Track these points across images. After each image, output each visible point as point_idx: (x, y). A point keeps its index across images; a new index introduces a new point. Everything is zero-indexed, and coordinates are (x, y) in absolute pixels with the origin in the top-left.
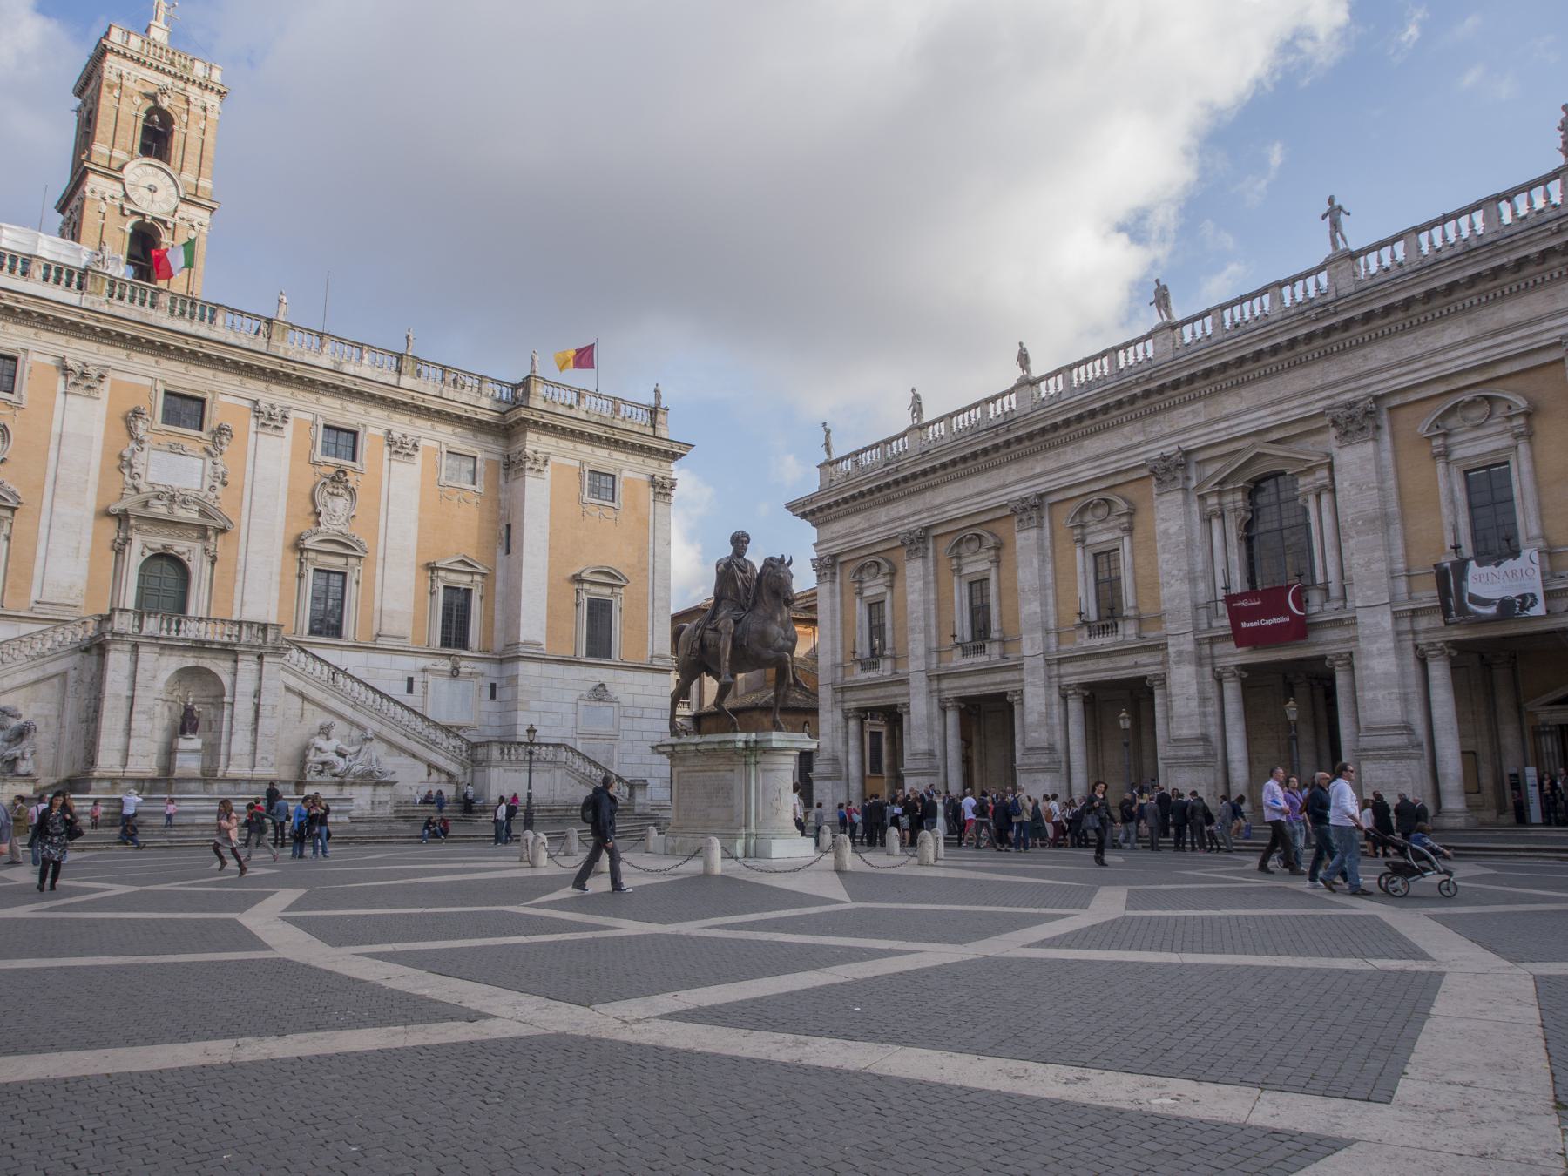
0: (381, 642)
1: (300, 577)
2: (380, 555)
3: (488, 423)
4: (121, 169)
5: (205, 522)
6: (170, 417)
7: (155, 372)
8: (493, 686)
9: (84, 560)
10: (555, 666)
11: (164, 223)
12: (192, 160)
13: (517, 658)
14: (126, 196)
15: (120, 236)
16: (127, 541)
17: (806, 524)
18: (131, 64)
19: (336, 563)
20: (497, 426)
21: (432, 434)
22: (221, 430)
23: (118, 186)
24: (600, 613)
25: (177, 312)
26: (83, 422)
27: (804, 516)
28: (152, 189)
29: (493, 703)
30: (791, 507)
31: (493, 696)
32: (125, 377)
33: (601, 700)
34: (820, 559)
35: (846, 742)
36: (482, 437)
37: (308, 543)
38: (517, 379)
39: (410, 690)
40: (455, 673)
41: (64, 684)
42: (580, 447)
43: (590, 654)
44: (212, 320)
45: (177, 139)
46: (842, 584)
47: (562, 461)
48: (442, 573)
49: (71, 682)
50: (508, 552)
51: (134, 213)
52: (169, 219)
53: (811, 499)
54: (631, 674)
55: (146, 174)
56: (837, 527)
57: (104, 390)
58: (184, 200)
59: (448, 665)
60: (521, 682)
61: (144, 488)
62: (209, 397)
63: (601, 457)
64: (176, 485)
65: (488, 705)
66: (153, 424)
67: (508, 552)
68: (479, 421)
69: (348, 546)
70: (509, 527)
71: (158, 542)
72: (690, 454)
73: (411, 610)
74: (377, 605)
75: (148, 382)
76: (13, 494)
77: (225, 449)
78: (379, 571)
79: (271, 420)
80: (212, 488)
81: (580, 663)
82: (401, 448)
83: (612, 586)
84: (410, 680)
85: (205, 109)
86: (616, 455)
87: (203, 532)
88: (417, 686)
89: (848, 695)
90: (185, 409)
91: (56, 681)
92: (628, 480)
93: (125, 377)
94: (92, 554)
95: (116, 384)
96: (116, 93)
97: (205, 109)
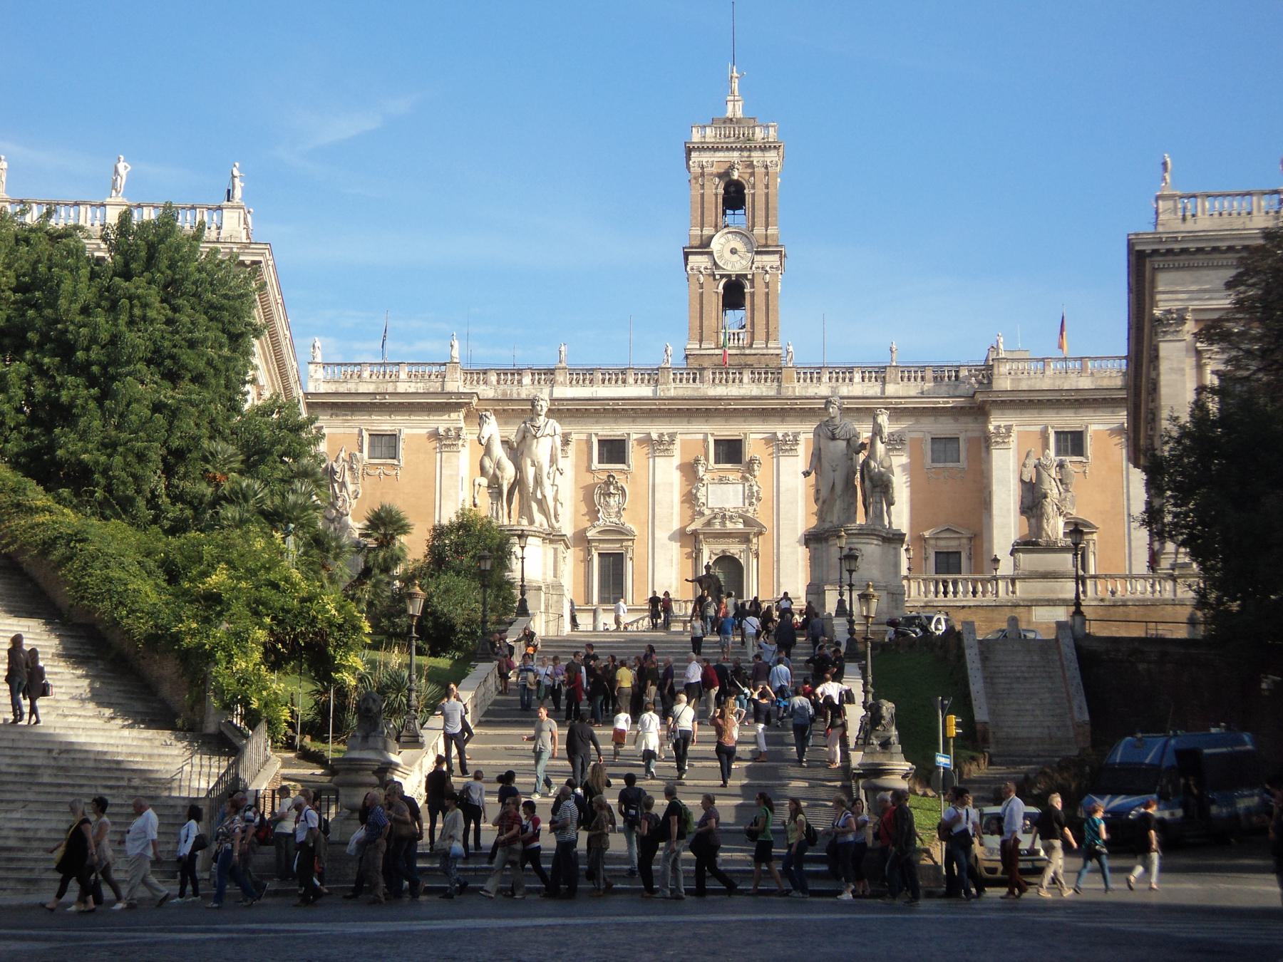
3: (962, 408)
4: (708, 245)
5: (748, 530)
11: (746, 276)
12: (760, 214)
14: (715, 264)
15: (715, 297)
18: (708, 154)
22: (752, 461)
25: (717, 381)
26: (668, 472)
28: (734, 251)
32: (689, 437)
36: (962, 419)
44: (741, 381)
45: (748, 199)
48: (932, 542)
51: (722, 276)
55: (728, 241)
57: (677, 449)
58: (758, 253)
61: (707, 512)
63: (1069, 420)
64: (727, 506)
66: (710, 468)
71: (719, 548)
76: (631, 532)
77: (757, 473)
80: (751, 504)
85: (766, 167)
87: (745, 538)
90: (731, 451)
97: (766, 167)
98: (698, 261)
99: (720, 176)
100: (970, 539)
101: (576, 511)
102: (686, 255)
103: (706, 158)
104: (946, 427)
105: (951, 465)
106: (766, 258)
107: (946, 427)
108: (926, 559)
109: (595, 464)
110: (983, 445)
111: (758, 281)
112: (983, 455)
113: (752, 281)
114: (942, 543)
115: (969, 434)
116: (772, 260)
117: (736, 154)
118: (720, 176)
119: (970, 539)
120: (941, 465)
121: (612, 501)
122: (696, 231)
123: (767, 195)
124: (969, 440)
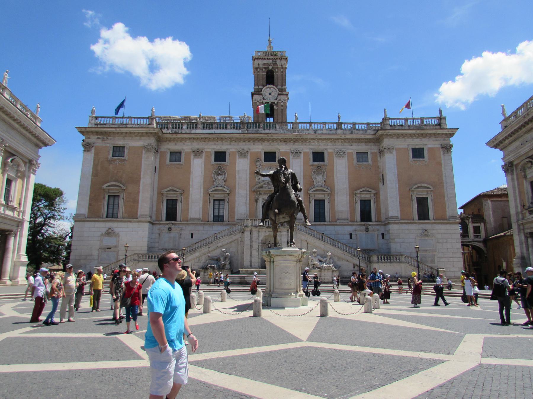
0: (338, 222)
1: (310, 203)
2: (336, 192)
3: (370, 139)
4: (261, 91)
6: (266, 160)
7: (261, 147)
8: (383, 235)
9: (248, 206)
10: (405, 225)
11: (274, 102)
13: (388, 223)
14: (263, 98)
16: (258, 198)
17: (497, 150)
18: (261, 60)
19: (320, 197)
20: (373, 139)
21: (351, 147)
23: (261, 96)
24: (422, 203)
27: (496, 147)
28: (270, 94)
29: (383, 240)
30: (488, 144)
31: (383, 238)
33: (427, 236)
34: (505, 165)
35: (527, 249)
37: (310, 192)
38: (380, 121)
39: (351, 237)
40: (367, 230)
41: (238, 242)
42: (407, 139)
43: (419, 219)
44: (276, 127)
45: (275, 77)
46: (517, 175)
47: (400, 147)
48: (359, 195)
49: (239, 242)
50: (383, 184)
51: (266, 103)
52: (276, 101)
53: (495, 138)
54: (440, 225)
56: (510, 148)
58: (279, 94)
59: (364, 228)
60: (391, 232)
62: (277, 151)
65: (381, 241)
67: (383, 184)
68: (367, 139)
69: (324, 191)
70: (383, 175)
72: (457, 133)
73: (349, 210)
74: (336, 209)
75: (259, 150)
78: (336, 198)
79: (296, 154)
81: (416, 223)
82: (340, 154)
83: (427, 191)
84: (351, 235)
85: (282, 65)
86: (423, 139)
88: (353, 236)
89: (526, 226)
91: (236, 241)
92: (429, 149)
93: (253, 151)
94: (249, 204)
95: (251, 153)
96: (258, 70)
98: (257, 97)
99: (265, 68)
100: (375, 194)
101: (205, 182)
102: (253, 95)
103: (261, 62)
104: (362, 148)
105: (365, 163)
106: (282, 96)
107: (362, 148)
108: (356, 203)
109: (213, 162)
110: (378, 155)
111: (279, 104)
112: (379, 159)
113: (277, 104)
114: (363, 196)
115: (373, 151)
116: (283, 97)
117: (271, 61)
118: (265, 68)
119: (375, 194)
120: (361, 163)
121: (220, 177)
122: (257, 87)
123: (282, 75)
124: (372, 153)
